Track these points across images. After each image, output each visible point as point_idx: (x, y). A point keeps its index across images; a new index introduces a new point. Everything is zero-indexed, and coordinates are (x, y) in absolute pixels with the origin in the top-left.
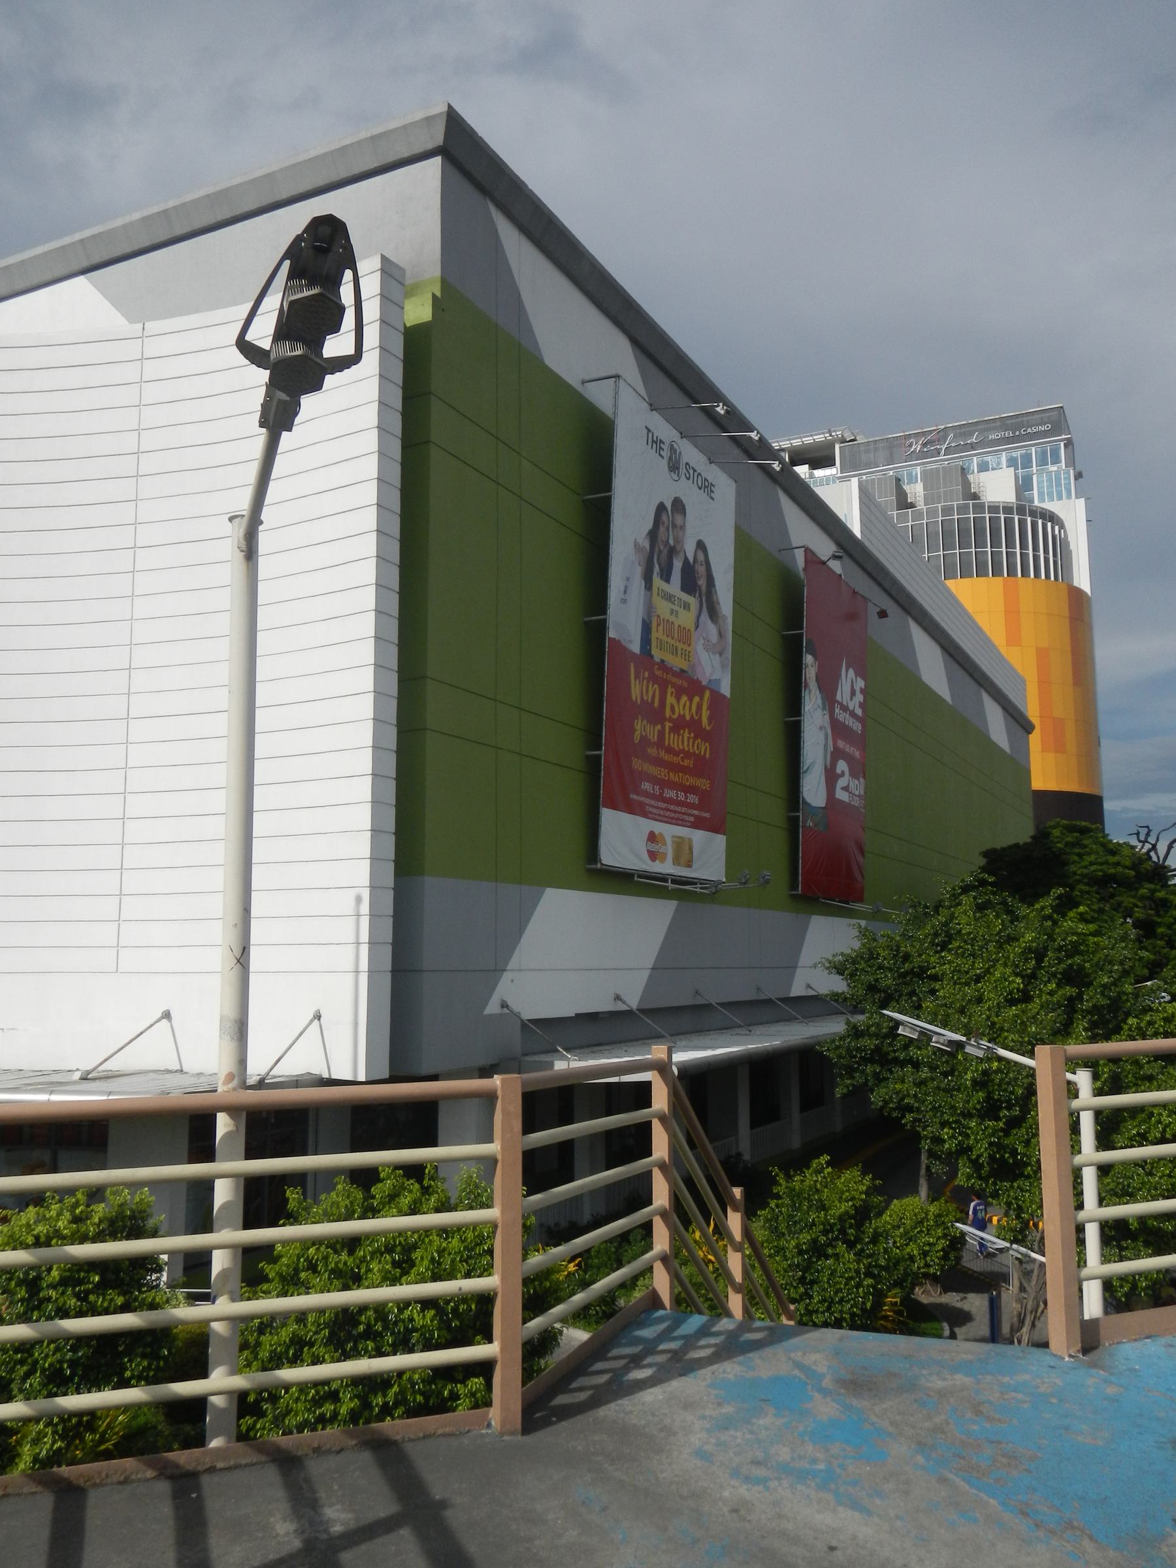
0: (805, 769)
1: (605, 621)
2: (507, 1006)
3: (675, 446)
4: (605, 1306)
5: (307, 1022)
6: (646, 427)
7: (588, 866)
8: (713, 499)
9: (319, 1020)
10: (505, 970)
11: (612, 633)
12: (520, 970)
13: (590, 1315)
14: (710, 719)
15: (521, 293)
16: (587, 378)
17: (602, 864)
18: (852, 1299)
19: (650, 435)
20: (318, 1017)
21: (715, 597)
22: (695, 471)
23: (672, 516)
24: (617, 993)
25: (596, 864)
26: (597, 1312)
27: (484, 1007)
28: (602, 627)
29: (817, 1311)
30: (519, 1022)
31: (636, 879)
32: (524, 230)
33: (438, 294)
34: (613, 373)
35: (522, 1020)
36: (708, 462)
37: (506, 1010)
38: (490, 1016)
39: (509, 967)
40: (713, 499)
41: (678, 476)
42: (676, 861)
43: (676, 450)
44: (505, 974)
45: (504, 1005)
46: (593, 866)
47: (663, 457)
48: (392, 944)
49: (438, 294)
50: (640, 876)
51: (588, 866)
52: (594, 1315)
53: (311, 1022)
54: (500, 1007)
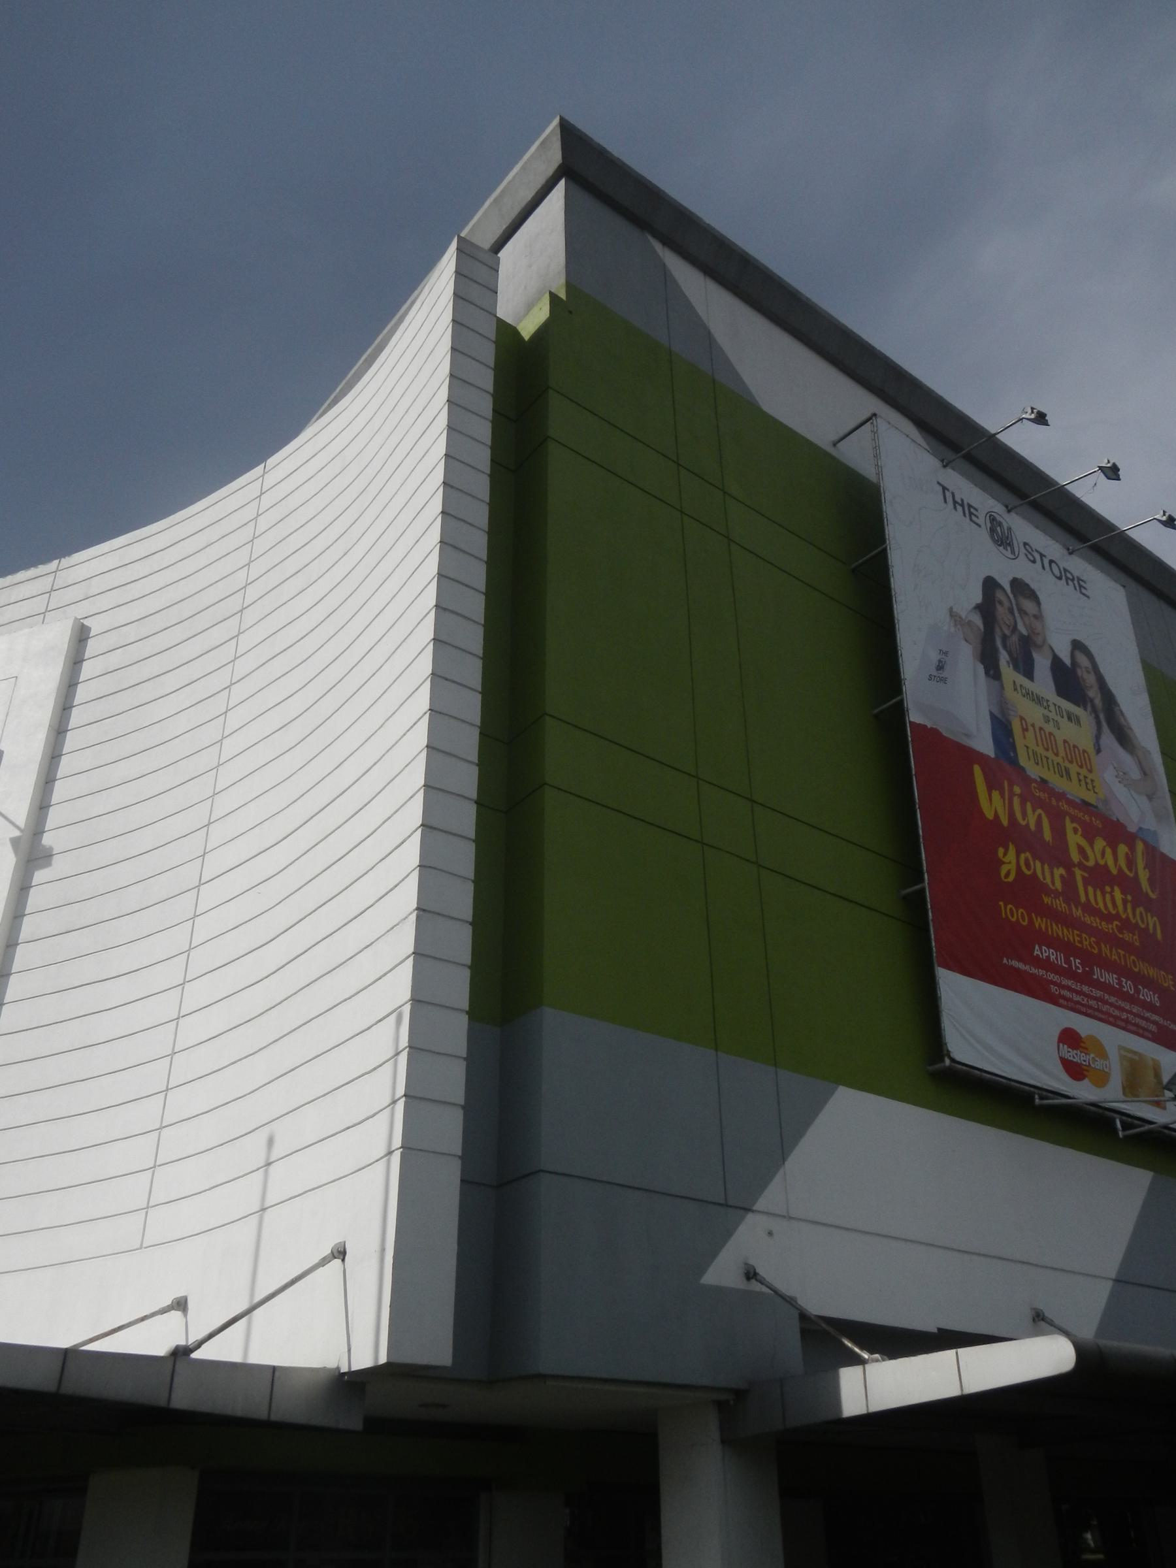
1: (901, 703)
3: (999, 518)
5: (316, 1260)
6: (938, 483)
7: (930, 1068)
8: (1088, 597)
9: (343, 1260)
10: (748, 1210)
11: (914, 716)
12: (791, 1218)
14: (1151, 881)
15: (712, 331)
16: (835, 437)
17: (953, 1060)
19: (948, 494)
20: (340, 1253)
21: (1122, 719)
22: (1042, 556)
23: (1016, 600)
24: (1040, 1306)
25: (943, 1061)
27: (702, 1270)
28: (899, 710)
30: (796, 1314)
31: (1037, 1101)
32: (709, 271)
33: (562, 295)
34: (867, 415)
35: (804, 1316)
36: (1065, 552)
37: (755, 1286)
38: (718, 1290)
39: (761, 1204)
40: (1088, 597)
41: (1013, 552)
42: (1131, 1087)
43: (1000, 524)
44: (750, 1217)
45: (751, 1275)
46: (938, 1066)
47: (979, 526)
48: (463, 1107)
49: (562, 295)
50: (1041, 1098)
51: (930, 1068)
53: (324, 1262)
54: (744, 1279)
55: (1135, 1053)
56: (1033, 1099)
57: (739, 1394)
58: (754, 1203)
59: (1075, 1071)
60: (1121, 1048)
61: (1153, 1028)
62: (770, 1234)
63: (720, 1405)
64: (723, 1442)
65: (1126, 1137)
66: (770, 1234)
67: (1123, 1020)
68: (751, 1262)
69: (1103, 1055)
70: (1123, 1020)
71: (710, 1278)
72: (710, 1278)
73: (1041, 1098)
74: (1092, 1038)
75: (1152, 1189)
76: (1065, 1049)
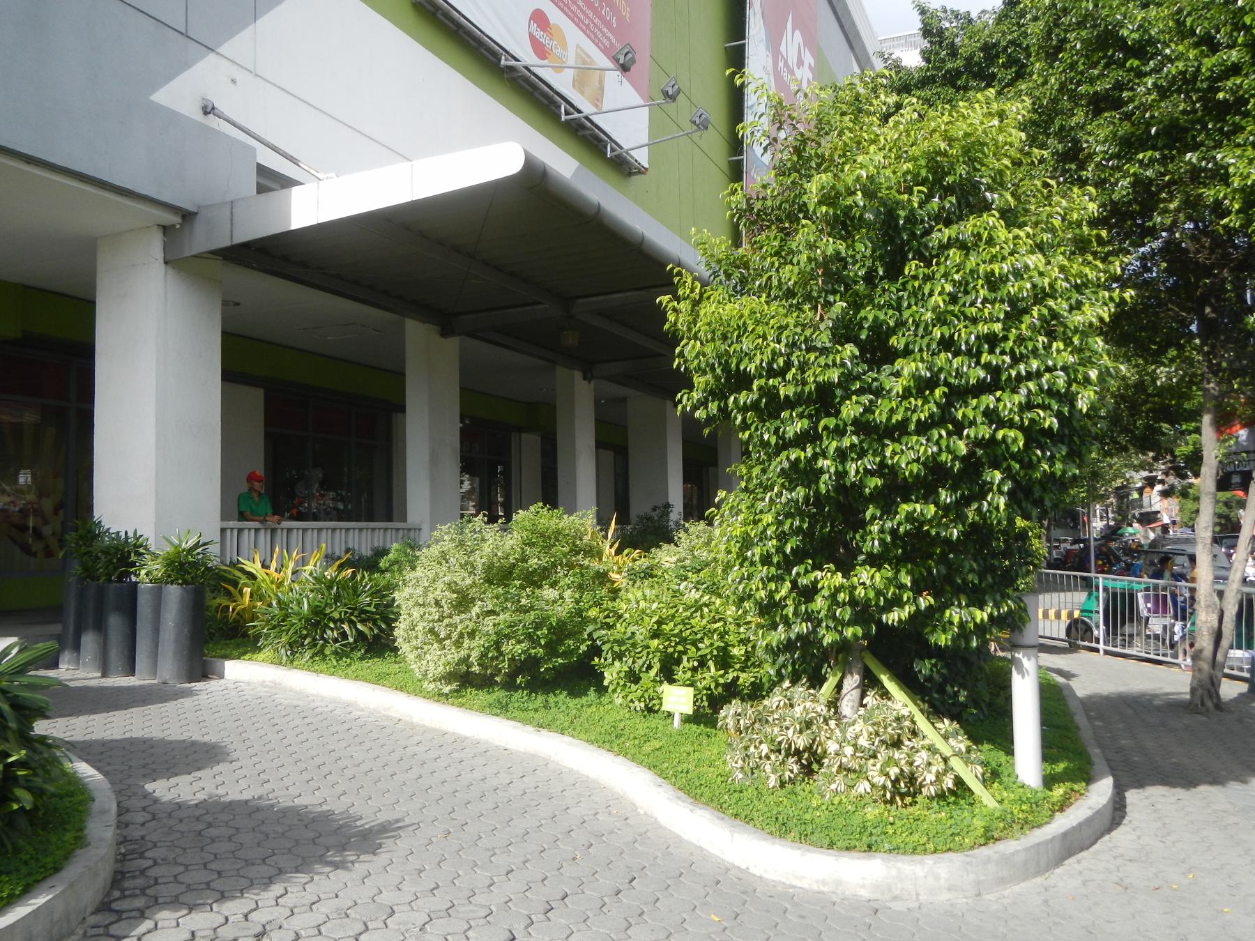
0: (749, 104)
2: (213, 108)
4: (363, 621)
12: (256, 75)
13: (326, 641)
18: (1029, 376)
26: (344, 635)
27: (156, 87)
29: (902, 427)
31: (503, 62)
37: (212, 121)
38: (171, 117)
44: (212, 56)
45: (208, 110)
52: (336, 641)
54: (201, 113)
55: (589, 56)
56: (499, 60)
57: (187, 216)
58: (220, 45)
59: (540, 50)
60: (578, 46)
61: (607, 44)
62: (234, 81)
63: (165, 229)
64: (166, 263)
65: (566, 121)
66: (234, 81)
67: (585, 24)
68: (209, 97)
69: (564, 45)
70: (585, 24)
71: (161, 97)
72: (161, 97)
73: (506, 60)
74: (558, 27)
75: (577, 170)
76: (534, 27)
